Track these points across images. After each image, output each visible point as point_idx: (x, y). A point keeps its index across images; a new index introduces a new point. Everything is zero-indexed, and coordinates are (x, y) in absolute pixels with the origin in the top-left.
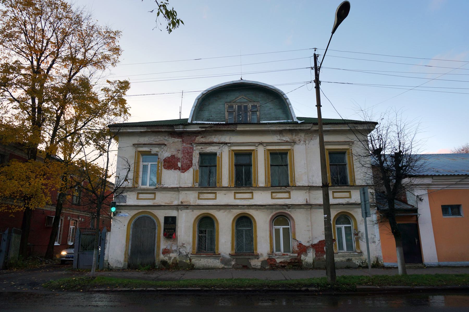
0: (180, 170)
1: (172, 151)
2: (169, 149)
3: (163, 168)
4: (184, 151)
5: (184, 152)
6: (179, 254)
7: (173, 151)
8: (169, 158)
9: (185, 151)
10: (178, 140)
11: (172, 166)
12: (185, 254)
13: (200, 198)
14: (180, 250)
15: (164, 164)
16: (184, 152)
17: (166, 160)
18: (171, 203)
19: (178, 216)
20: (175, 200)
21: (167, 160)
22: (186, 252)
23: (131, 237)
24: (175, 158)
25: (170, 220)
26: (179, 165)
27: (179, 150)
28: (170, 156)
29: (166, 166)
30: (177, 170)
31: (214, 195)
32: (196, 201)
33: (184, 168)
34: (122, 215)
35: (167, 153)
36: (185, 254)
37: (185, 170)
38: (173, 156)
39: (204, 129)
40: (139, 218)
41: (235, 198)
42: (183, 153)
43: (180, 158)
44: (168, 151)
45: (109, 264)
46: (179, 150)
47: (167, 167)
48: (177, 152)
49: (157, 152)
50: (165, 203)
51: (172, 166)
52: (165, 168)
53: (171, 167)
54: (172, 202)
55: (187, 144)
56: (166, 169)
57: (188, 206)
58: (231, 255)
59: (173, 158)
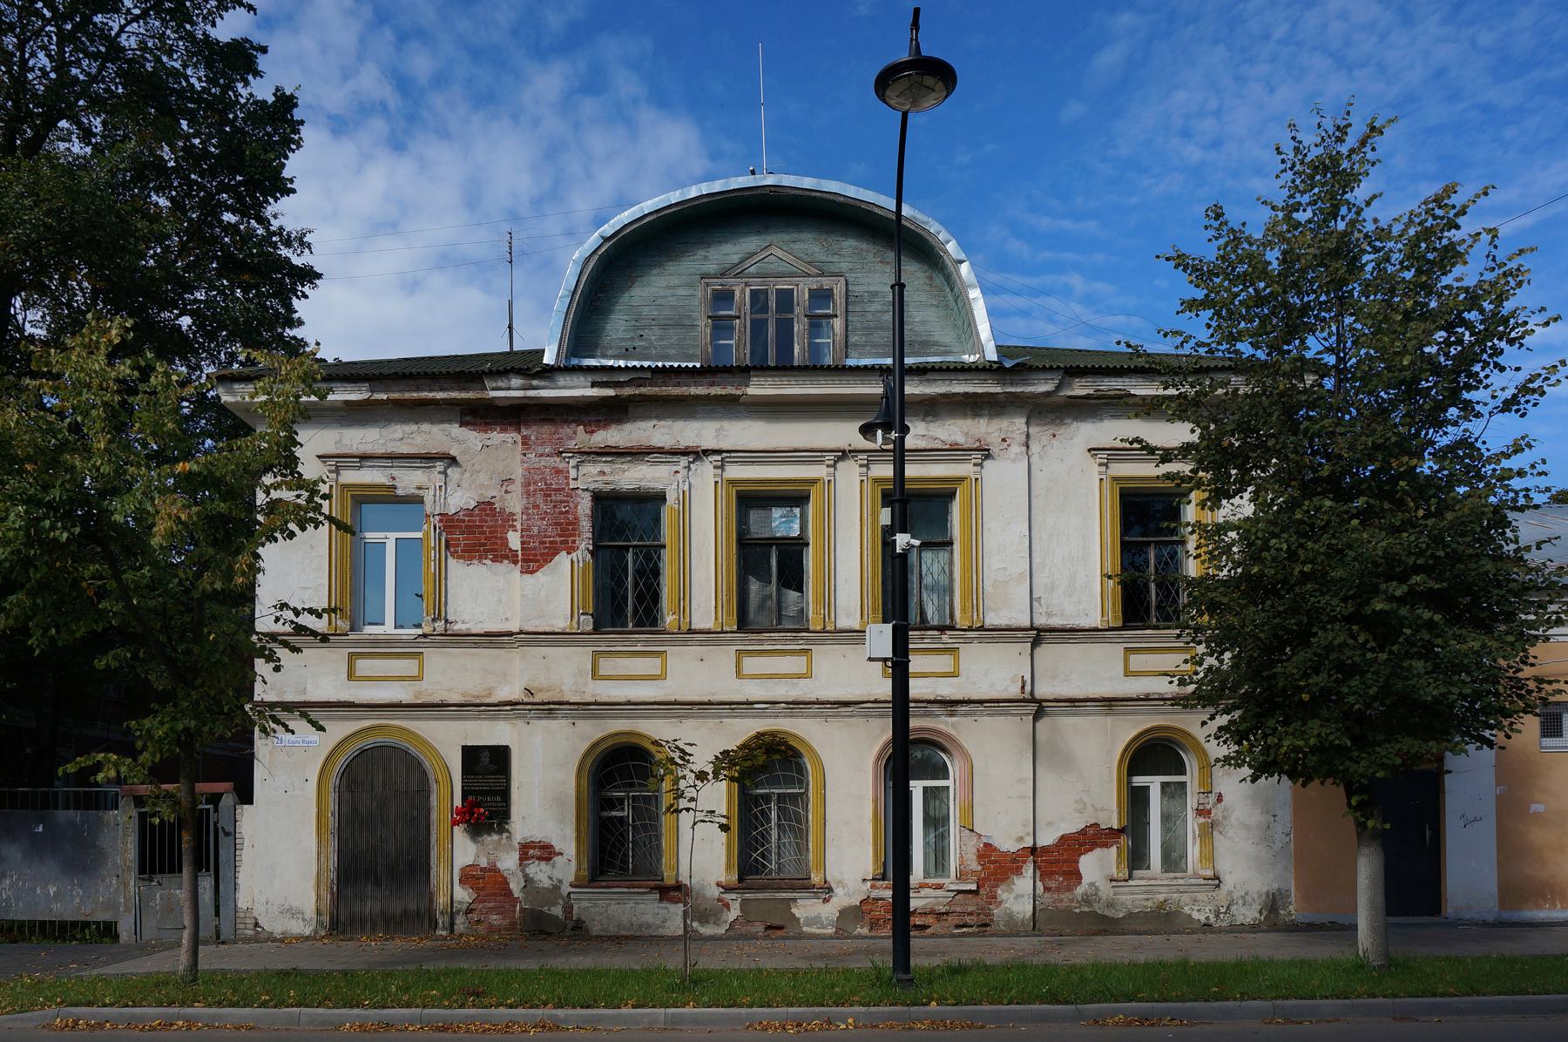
1: (482, 486)
4: (529, 484)
5: (532, 488)
6: (525, 887)
8: (472, 515)
11: (485, 545)
12: (546, 886)
13: (602, 672)
16: (532, 488)
22: (551, 878)
23: (332, 823)
24: (495, 515)
25: (485, 758)
26: (514, 541)
28: (472, 504)
30: (506, 562)
31: (658, 661)
32: (587, 683)
33: (535, 555)
34: (293, 742)
36: (547, 883)
38: (486, 507)
39: (610, 392)
40: (363, 752)
41: (739, 674)
42: (528, 493)
43: (514, 515)
45: (257, 925)
47: (463, 551)
49: (420, 488)
50: (463, 695)
51: (485, 545)
57: (552, 706)
58: (723, 887)
59: (486, 515)
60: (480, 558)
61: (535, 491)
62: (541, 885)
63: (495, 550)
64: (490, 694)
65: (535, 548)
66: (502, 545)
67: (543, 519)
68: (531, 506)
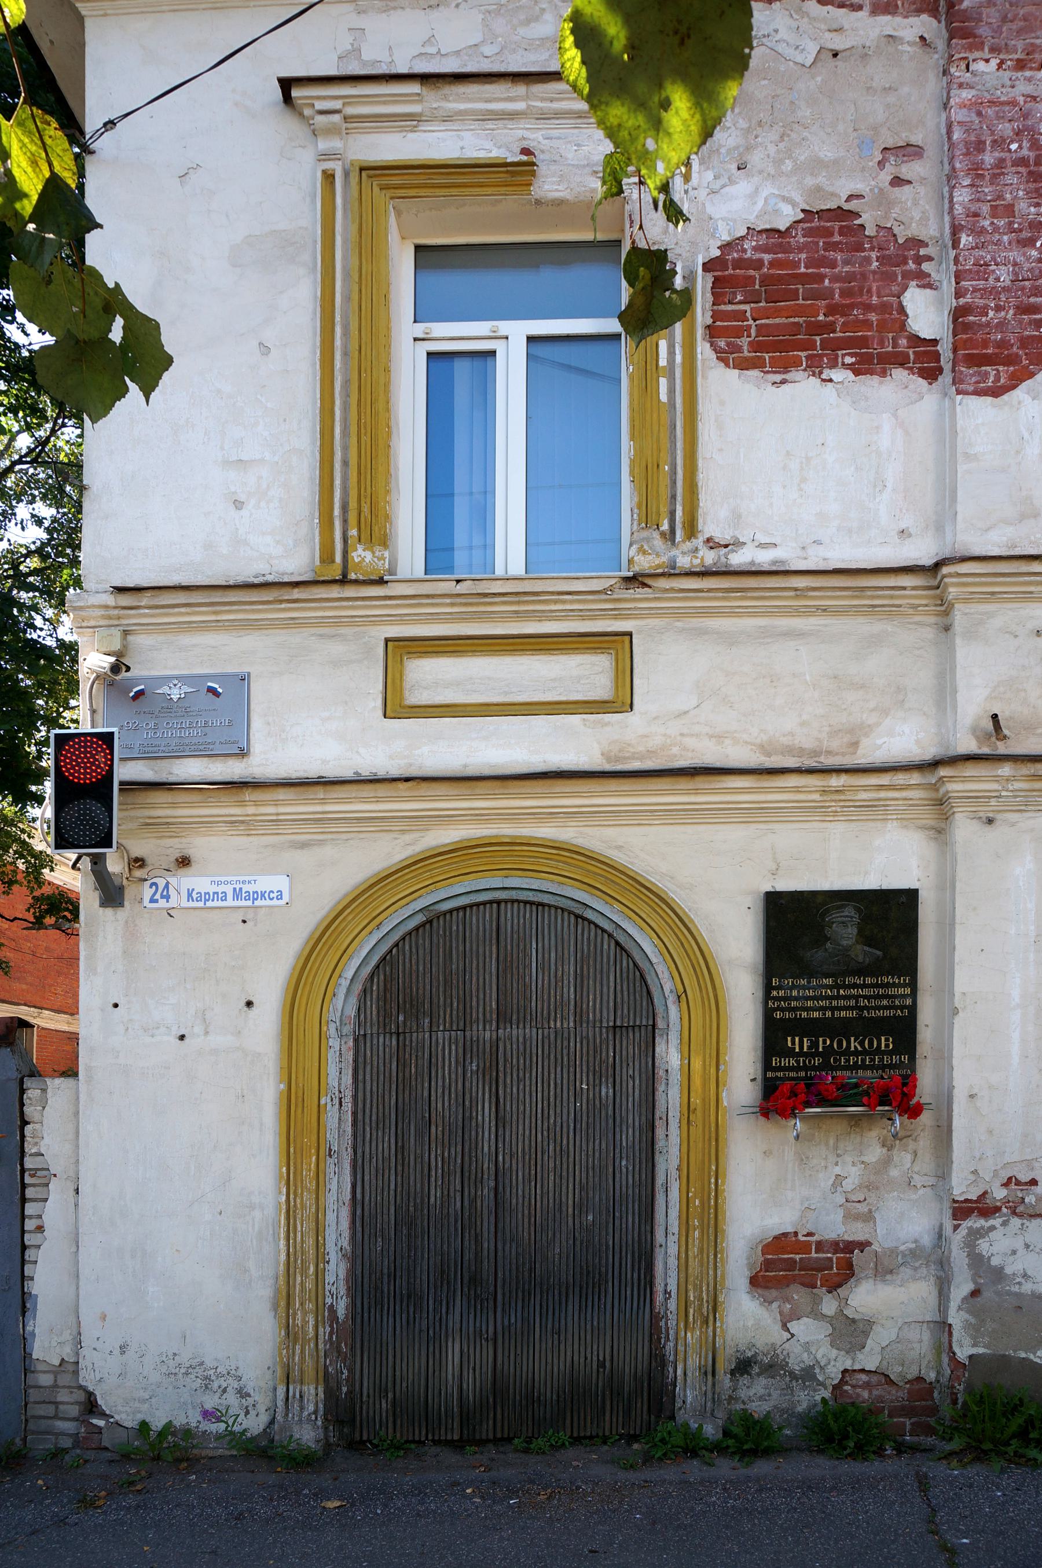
0: (931, 374)
1: (817, 164)
2: (768, 137)
3: (704, 350)
4: (979, 146)
5: (989, 158)
7: (827, 153)
8: (786, 249)
9: (1000, 143)
10: (886, 23)
11: (830, 327)
14: (983, 1246)
15: (716, 316)
16: (989, 158)
17: (739, 264)
18: (835, 744)
19: (947, 884)
20: (885, 712)
21: (758, 264)
24: (859, 248)
27: (910, 151)
28: (785, 216)
29: (738, 332)
30: (899, 374)
33: (1003, 344)
35: (743, 187)
37: (1009, 361)
42: (976, 171)
43: (922, 244)
44: (756, 159)
46: (910, 151)
47: (756, 347)
48: (885, 176)
51: (830, 327)
52: (728, 357)
53: (808, 346)
54: (855, 735)
55: (1020, 65)
56: (743, 365)
60: (815, 367)
61: (1000, 163)
62: (1027, 1288)
63: (864, 342)
64: (855, 744)
65: (1002, 325)
66: (882, 326)
67: (1030, 242)
68: (985, 209)
